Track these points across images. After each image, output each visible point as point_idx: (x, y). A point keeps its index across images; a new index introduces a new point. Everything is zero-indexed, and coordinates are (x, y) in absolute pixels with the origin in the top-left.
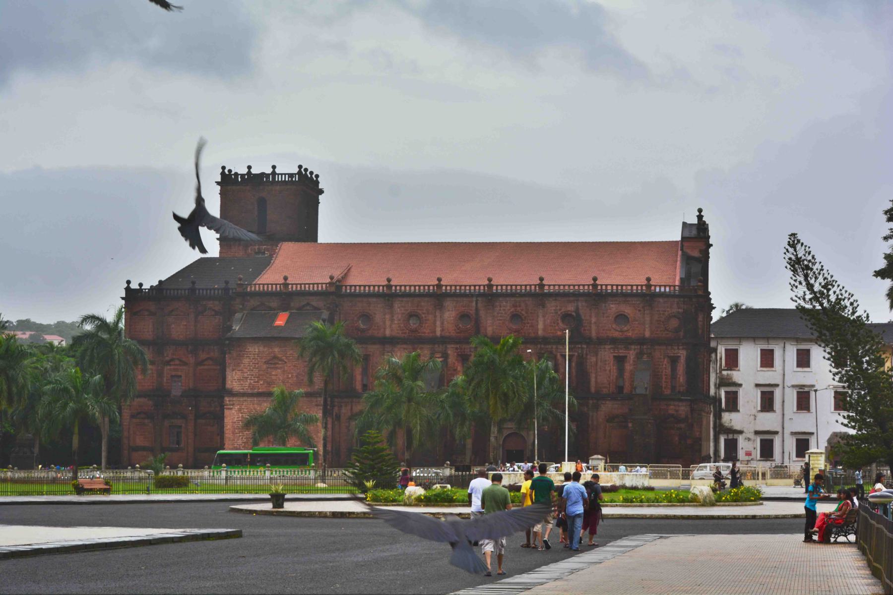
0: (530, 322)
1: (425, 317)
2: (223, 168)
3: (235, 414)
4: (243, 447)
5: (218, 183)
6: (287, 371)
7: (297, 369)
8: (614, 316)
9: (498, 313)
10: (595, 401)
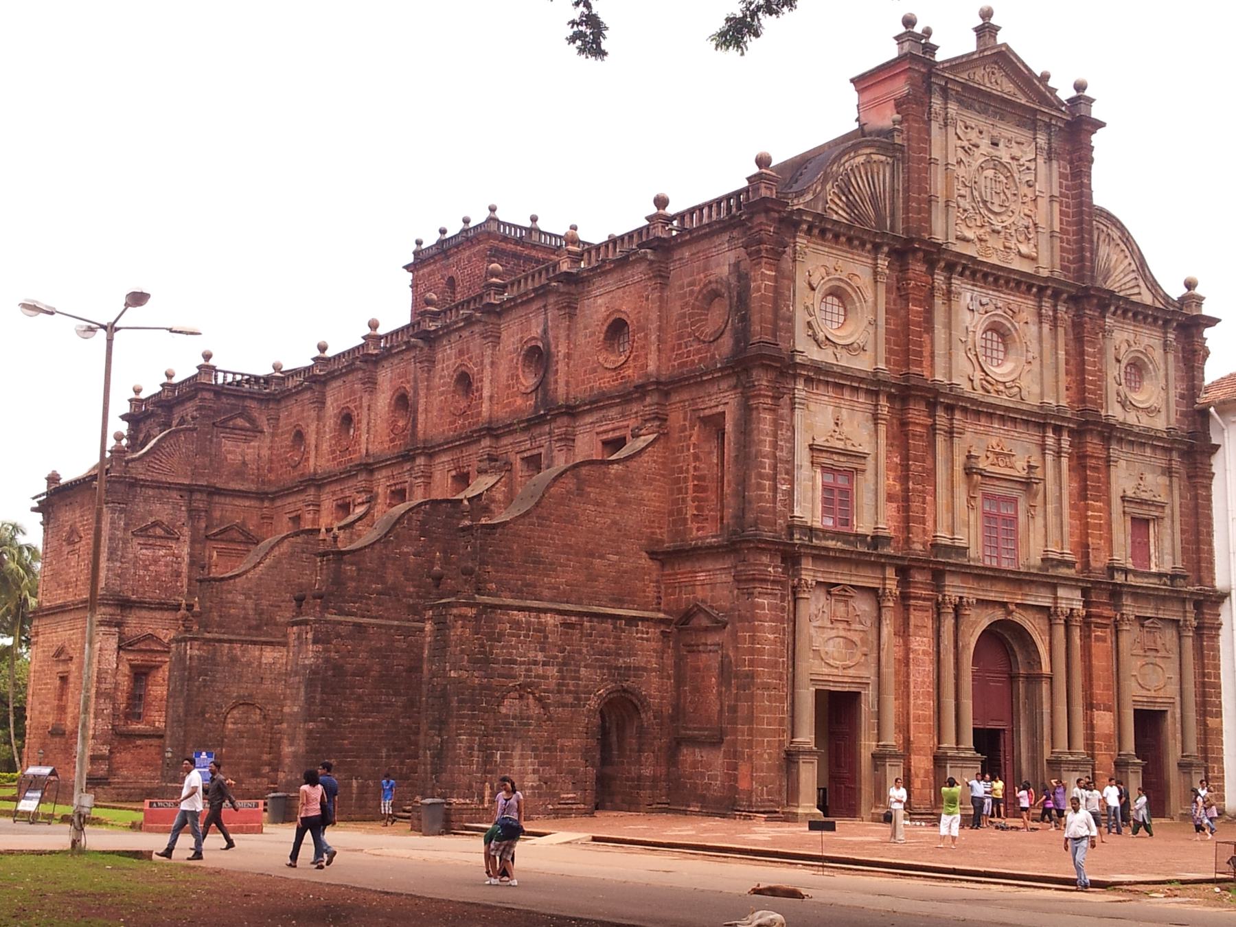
5: (407, 267)
8: (605, 328)
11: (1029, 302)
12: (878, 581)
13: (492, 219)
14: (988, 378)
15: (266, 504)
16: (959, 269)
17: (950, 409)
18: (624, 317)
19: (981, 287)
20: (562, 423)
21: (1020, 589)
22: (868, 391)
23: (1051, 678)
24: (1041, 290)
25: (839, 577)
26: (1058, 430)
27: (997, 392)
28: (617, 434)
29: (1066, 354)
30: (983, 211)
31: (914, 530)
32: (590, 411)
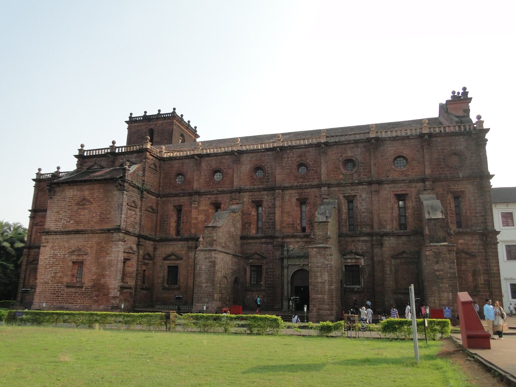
0: (314, 169)
1: (226, 171)
2: (131, 114)
3: (49, 251)
4: (51, 281)
5: (126, 122)
6: (93, 210)
7: (101, 209)
8: (394, 158)
9: (286, 164)
10: (379, 238)
13: (174, 112)
15: (159, 199)
18: (404, 155)
20: (374, 187)
28: (403, 192)
32: (388, 184)
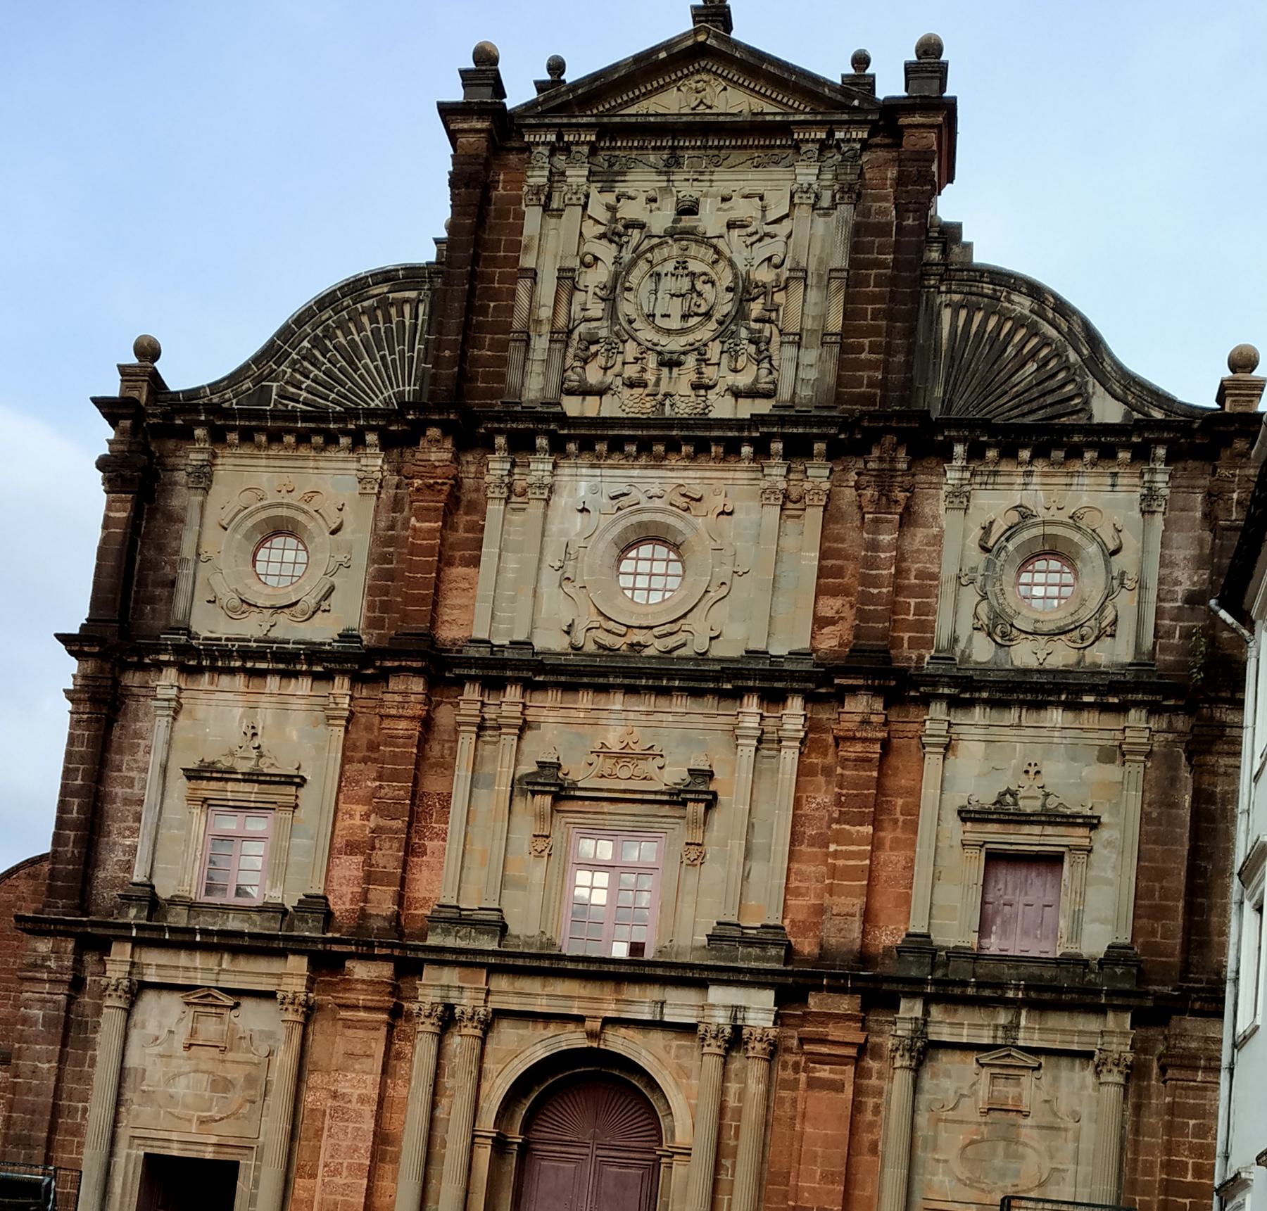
11: (739, 475)
12: (275, 981)
14: (611, 625)
16: (542, 442)
17: (494, 685)
19: (612, 467)
21: (617, 991)
22: (316, 677)
23: (689, 1155)
24: (762, 450)
25: (192, 974)
26: (773, 698)
27: (632, 645)
29: (823, 555)
30: (646, 334)
31: (371, 896)
